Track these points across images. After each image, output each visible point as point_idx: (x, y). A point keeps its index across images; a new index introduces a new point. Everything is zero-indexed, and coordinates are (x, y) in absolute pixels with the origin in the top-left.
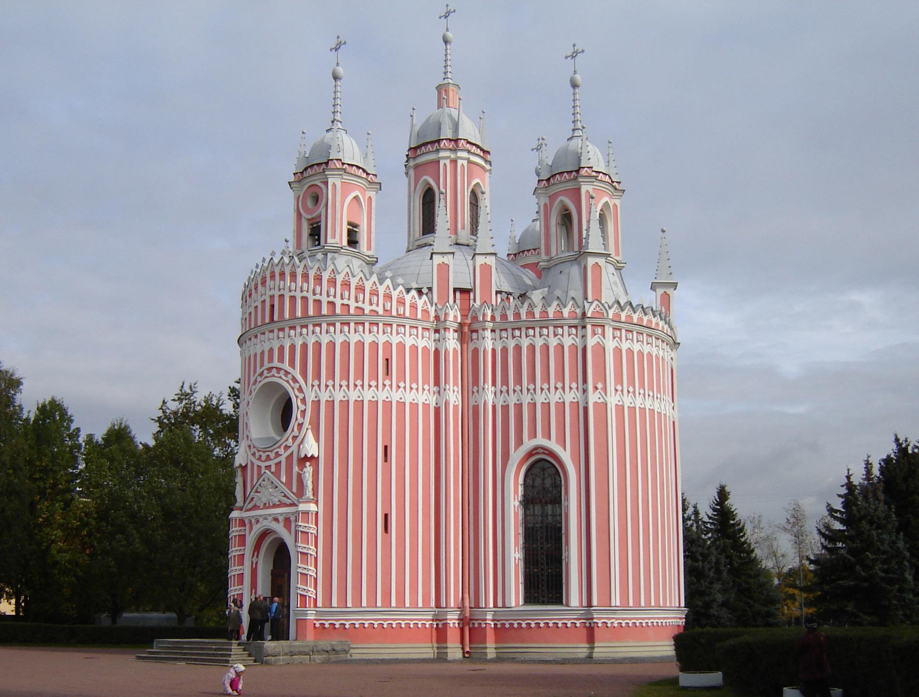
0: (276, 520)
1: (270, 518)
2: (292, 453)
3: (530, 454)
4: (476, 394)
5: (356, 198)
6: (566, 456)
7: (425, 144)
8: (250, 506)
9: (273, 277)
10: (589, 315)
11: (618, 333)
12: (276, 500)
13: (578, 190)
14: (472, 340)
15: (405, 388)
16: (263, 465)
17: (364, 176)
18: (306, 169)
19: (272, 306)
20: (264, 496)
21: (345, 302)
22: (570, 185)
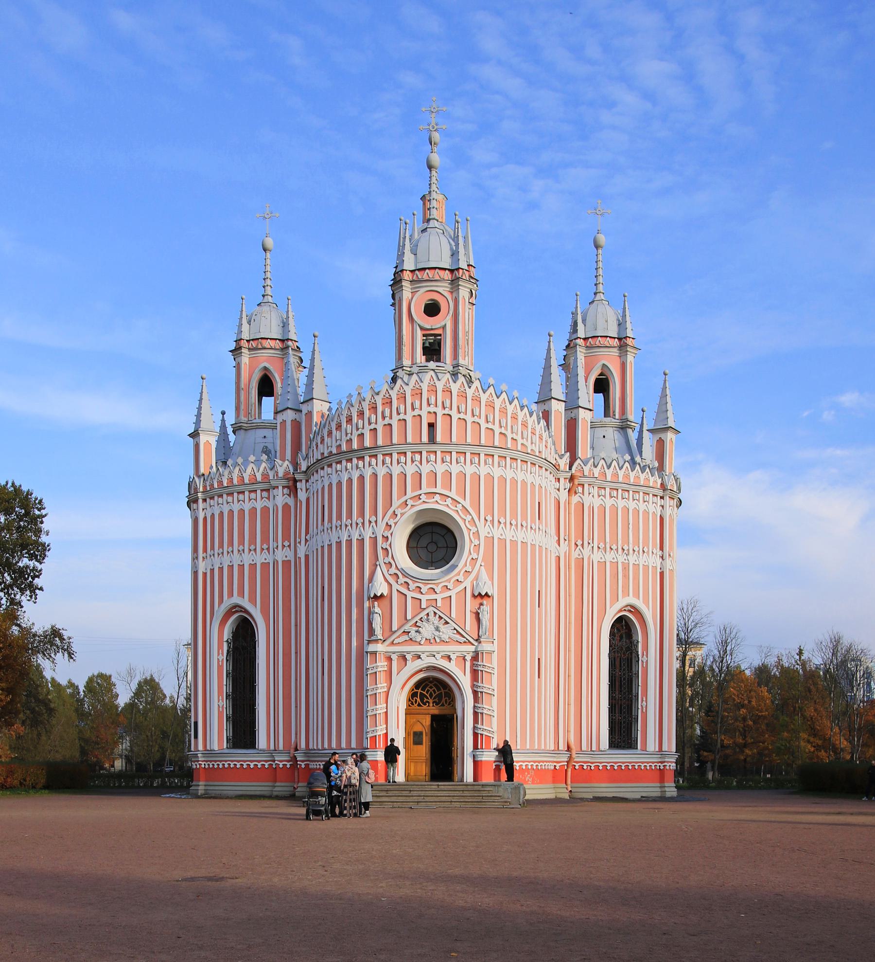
4: (580, 547)
12: (445, 637)
14: (576, 493)
20: (427, 630)
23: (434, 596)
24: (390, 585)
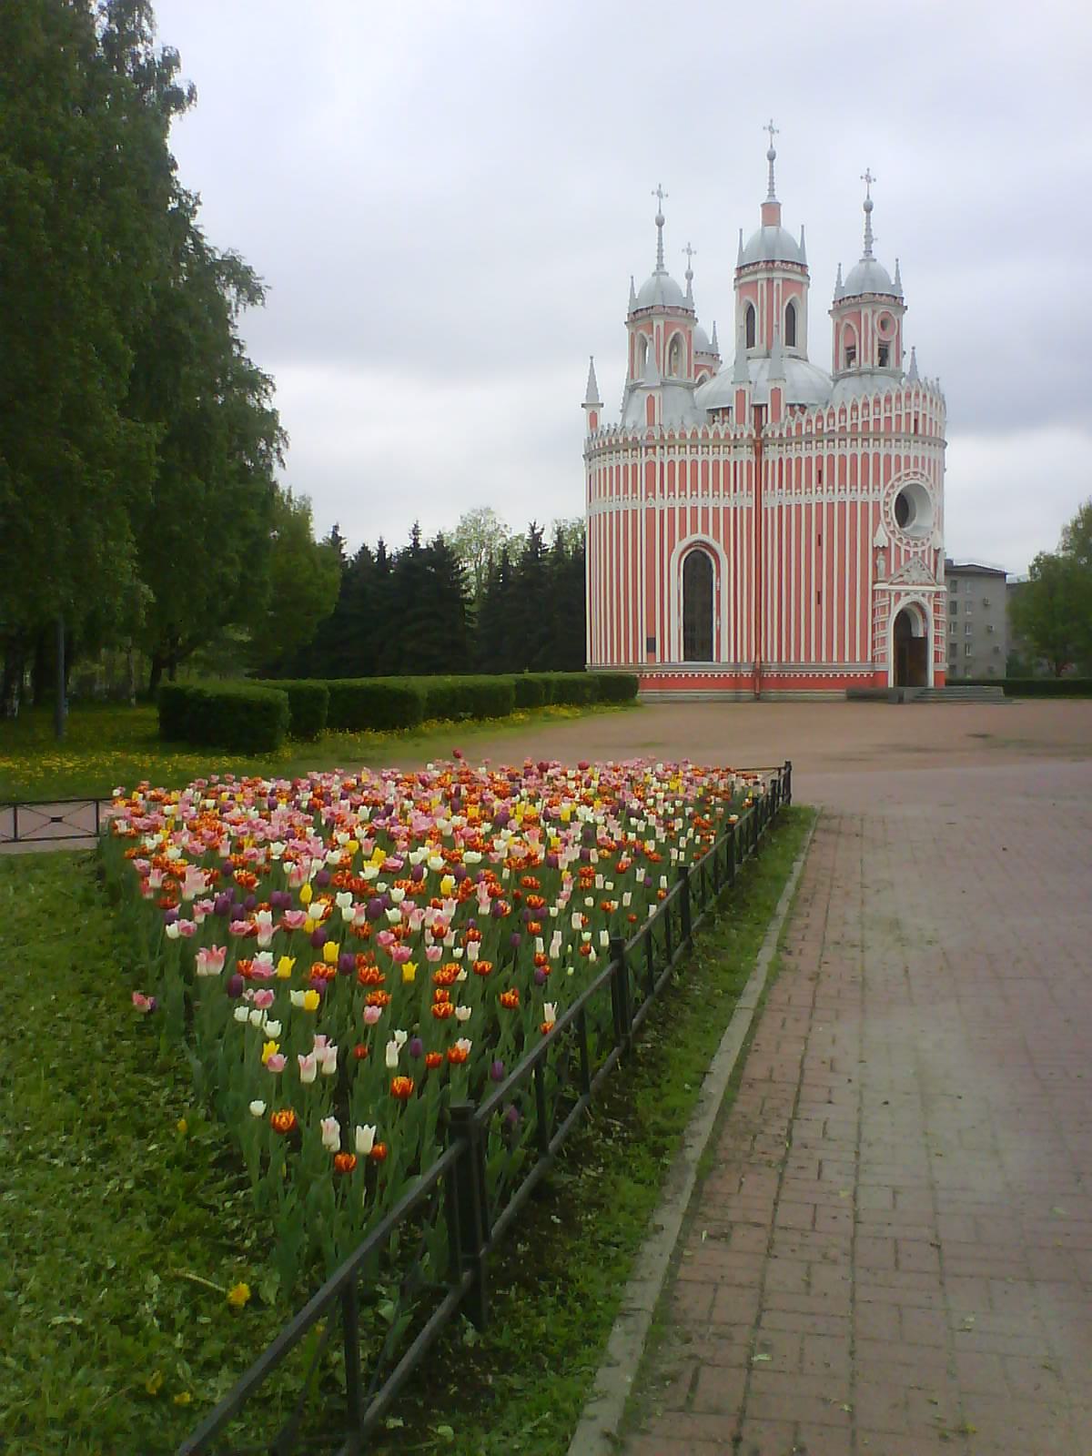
0: (923, 595)
19: (916, 421)
20: (914, 575)
23: (915, 550)
24: (890, 539)
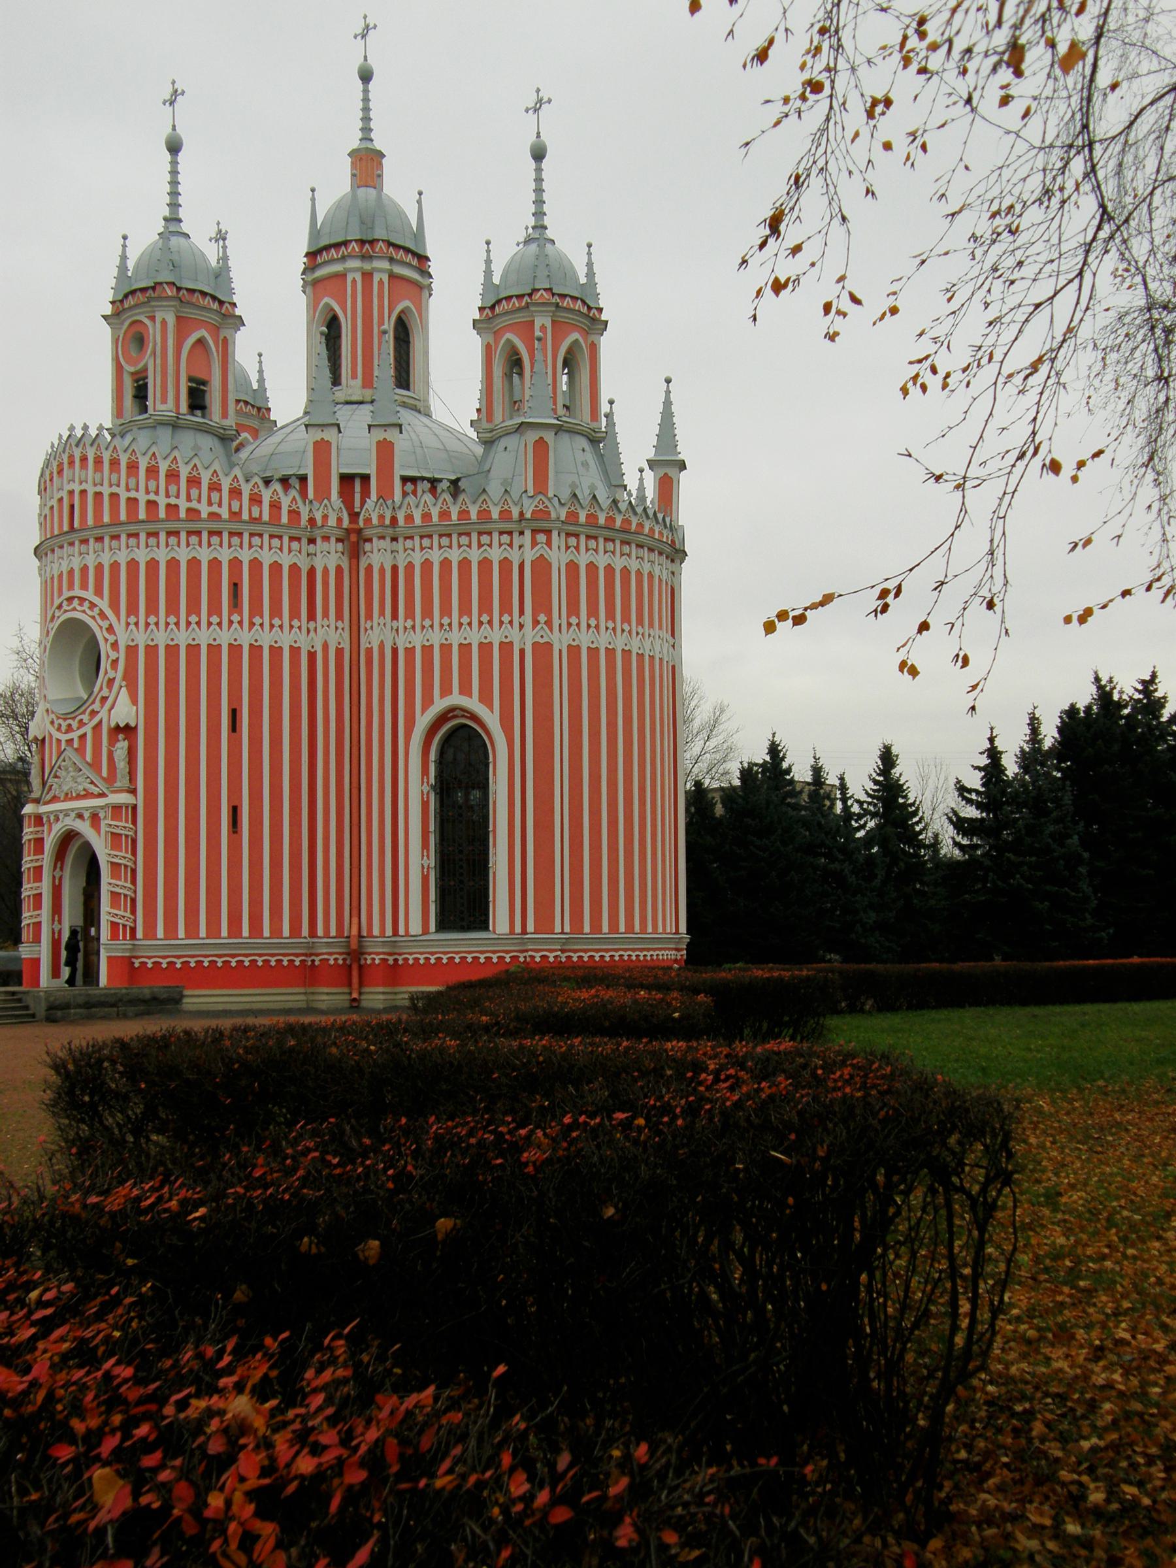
0: (80, 816)
1: (73, 815)
2: (101, 722)
3: (443, 718)
5: (200, 342)
6: (491, 719)
7: (327, 248)
8: (48, 797)
9: (71, 463)
10: (528, 516)
11: (573, 541)
13: (533, 322)
15: (262, 625)
16: (64, 737)
17: (216, 306)
18: (126, 296)
19: (72, 507)
20: (67, 782)
21: (173, 501)
22: (521, 317)
